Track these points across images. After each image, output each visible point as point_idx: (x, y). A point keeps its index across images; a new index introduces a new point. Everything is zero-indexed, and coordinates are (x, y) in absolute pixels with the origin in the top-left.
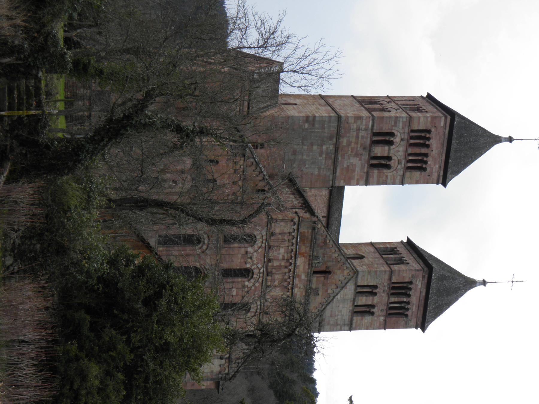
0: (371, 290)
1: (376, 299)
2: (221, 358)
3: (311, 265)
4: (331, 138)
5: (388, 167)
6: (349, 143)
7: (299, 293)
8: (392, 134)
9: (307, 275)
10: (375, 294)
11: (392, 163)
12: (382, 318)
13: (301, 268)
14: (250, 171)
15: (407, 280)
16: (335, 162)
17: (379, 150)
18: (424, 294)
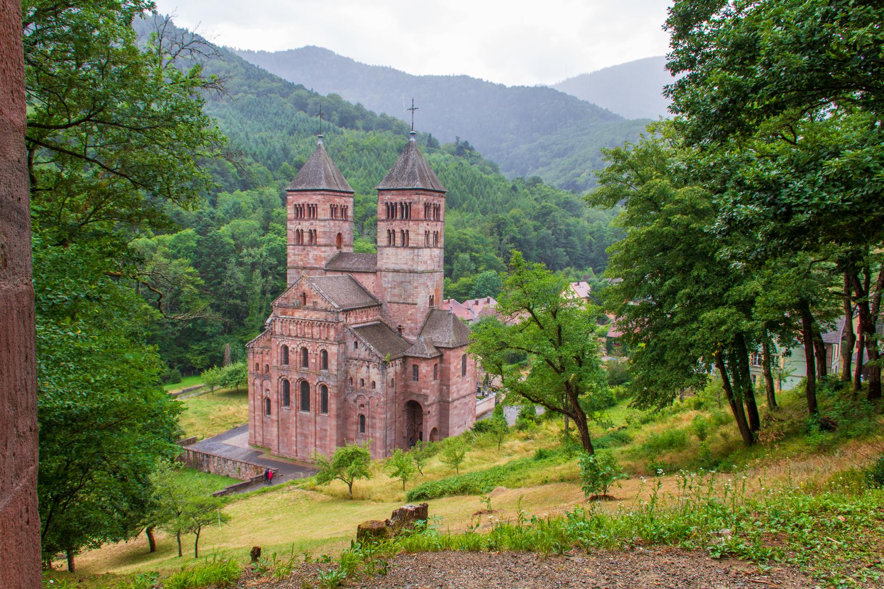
0: (391, 234)
1: (397, 230)
2: (368, 367)
3: (298, 308)
4: (299, 273)
5: (315, 231)
6: (302, 260)
7: (314, 316)
8: (298, 230)
9: (304, 309)
10: (394, 231)
11: (312, 229)
12: (411, 223)
13: (301, 314)
14: (261, 345)
15: (384, 207)
16: (312, 269)
17: (306, 239)
18: (394, 192)
